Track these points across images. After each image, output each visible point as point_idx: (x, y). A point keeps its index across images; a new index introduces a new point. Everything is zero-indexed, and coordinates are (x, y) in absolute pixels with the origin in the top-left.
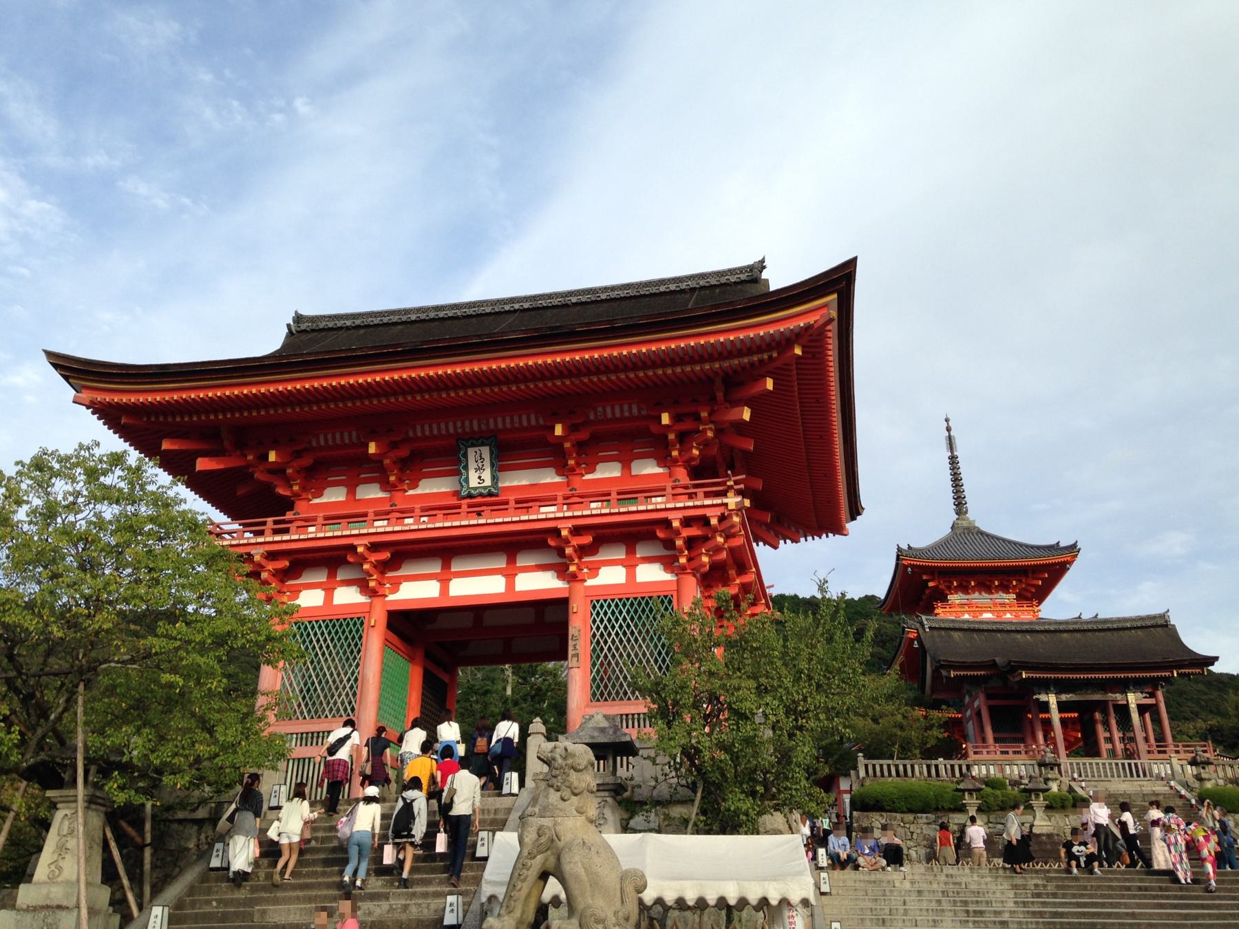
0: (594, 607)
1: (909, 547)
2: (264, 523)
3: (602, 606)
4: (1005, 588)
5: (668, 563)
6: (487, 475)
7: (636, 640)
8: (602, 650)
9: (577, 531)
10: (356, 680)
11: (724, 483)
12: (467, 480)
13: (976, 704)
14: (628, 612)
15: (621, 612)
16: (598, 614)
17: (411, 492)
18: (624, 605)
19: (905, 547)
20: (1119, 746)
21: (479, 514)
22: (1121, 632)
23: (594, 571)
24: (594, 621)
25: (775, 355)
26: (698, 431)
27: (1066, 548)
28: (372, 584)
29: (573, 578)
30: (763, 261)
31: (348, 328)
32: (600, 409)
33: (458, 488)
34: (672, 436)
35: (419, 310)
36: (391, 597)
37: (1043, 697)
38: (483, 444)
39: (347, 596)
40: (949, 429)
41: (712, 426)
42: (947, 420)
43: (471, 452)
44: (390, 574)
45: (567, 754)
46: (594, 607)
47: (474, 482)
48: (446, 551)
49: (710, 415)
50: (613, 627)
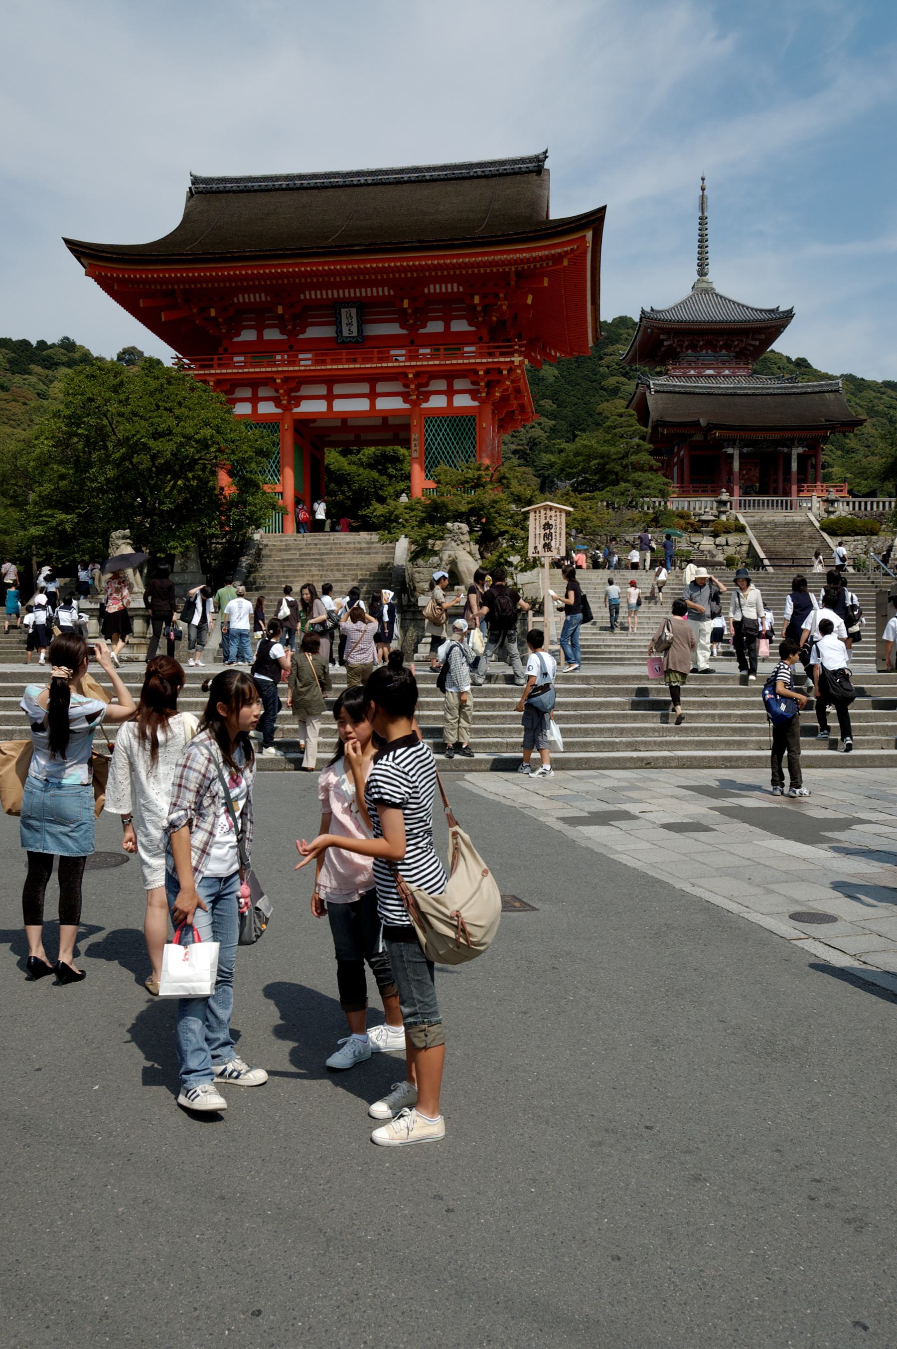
0: (427, 422)
1: (652, 310)
2: (212, 360)
3: (431, 422)
4: (727, 346)
5: (474, 394)
6: (354, 329)
7: (458, 452)
8: (432, 449)
9: (417, 375)
10: (278, 462)
11: (512, 346)
12: (341, 331)
13: (682, 453)
14: (448, 425)
15: (443, 426)
16: (429, 426)
17: (301, 336)
18: (446, 421)
19: (648, 309)
20: (781, 487)
21: (355, 361)
22: (802, 397)
23: (427, 396)
24: (427, 431)
25: (551, 264)
26: (496, 304)
27: (784, 312)
28: (284, 402)
29: (415, 404)
30: (546, 152)
31: (234, 192)
32: (432, 286)
33: (334, 335)
34: (479, 308)
35: (287, 178)
36: (296, 410)
37: (730, 451)
38: (352, 307)
39: (267, 408)
40: (703, 189)
41: (506, 302)
42: (703, 179)
43: (344, 311)
44: (293, 394)
45: (460, 528)
46: (427, 422)
47: (345, 333)
48: (330, 381)
49: (505, 295)
50: (439, 435)
